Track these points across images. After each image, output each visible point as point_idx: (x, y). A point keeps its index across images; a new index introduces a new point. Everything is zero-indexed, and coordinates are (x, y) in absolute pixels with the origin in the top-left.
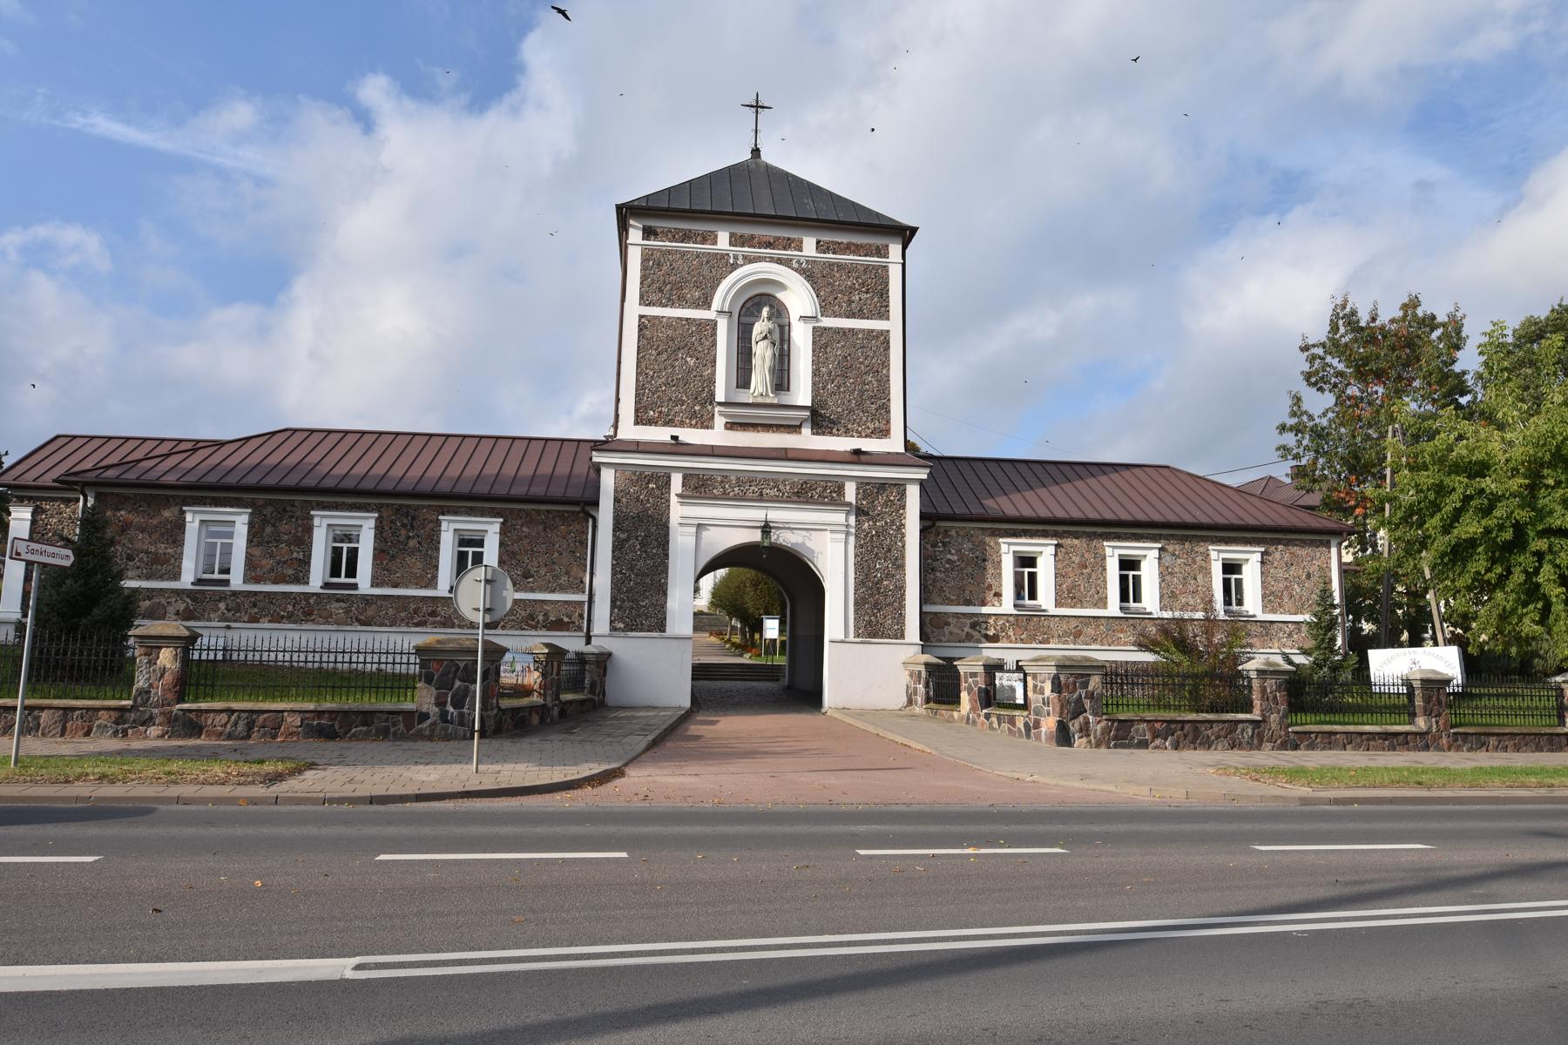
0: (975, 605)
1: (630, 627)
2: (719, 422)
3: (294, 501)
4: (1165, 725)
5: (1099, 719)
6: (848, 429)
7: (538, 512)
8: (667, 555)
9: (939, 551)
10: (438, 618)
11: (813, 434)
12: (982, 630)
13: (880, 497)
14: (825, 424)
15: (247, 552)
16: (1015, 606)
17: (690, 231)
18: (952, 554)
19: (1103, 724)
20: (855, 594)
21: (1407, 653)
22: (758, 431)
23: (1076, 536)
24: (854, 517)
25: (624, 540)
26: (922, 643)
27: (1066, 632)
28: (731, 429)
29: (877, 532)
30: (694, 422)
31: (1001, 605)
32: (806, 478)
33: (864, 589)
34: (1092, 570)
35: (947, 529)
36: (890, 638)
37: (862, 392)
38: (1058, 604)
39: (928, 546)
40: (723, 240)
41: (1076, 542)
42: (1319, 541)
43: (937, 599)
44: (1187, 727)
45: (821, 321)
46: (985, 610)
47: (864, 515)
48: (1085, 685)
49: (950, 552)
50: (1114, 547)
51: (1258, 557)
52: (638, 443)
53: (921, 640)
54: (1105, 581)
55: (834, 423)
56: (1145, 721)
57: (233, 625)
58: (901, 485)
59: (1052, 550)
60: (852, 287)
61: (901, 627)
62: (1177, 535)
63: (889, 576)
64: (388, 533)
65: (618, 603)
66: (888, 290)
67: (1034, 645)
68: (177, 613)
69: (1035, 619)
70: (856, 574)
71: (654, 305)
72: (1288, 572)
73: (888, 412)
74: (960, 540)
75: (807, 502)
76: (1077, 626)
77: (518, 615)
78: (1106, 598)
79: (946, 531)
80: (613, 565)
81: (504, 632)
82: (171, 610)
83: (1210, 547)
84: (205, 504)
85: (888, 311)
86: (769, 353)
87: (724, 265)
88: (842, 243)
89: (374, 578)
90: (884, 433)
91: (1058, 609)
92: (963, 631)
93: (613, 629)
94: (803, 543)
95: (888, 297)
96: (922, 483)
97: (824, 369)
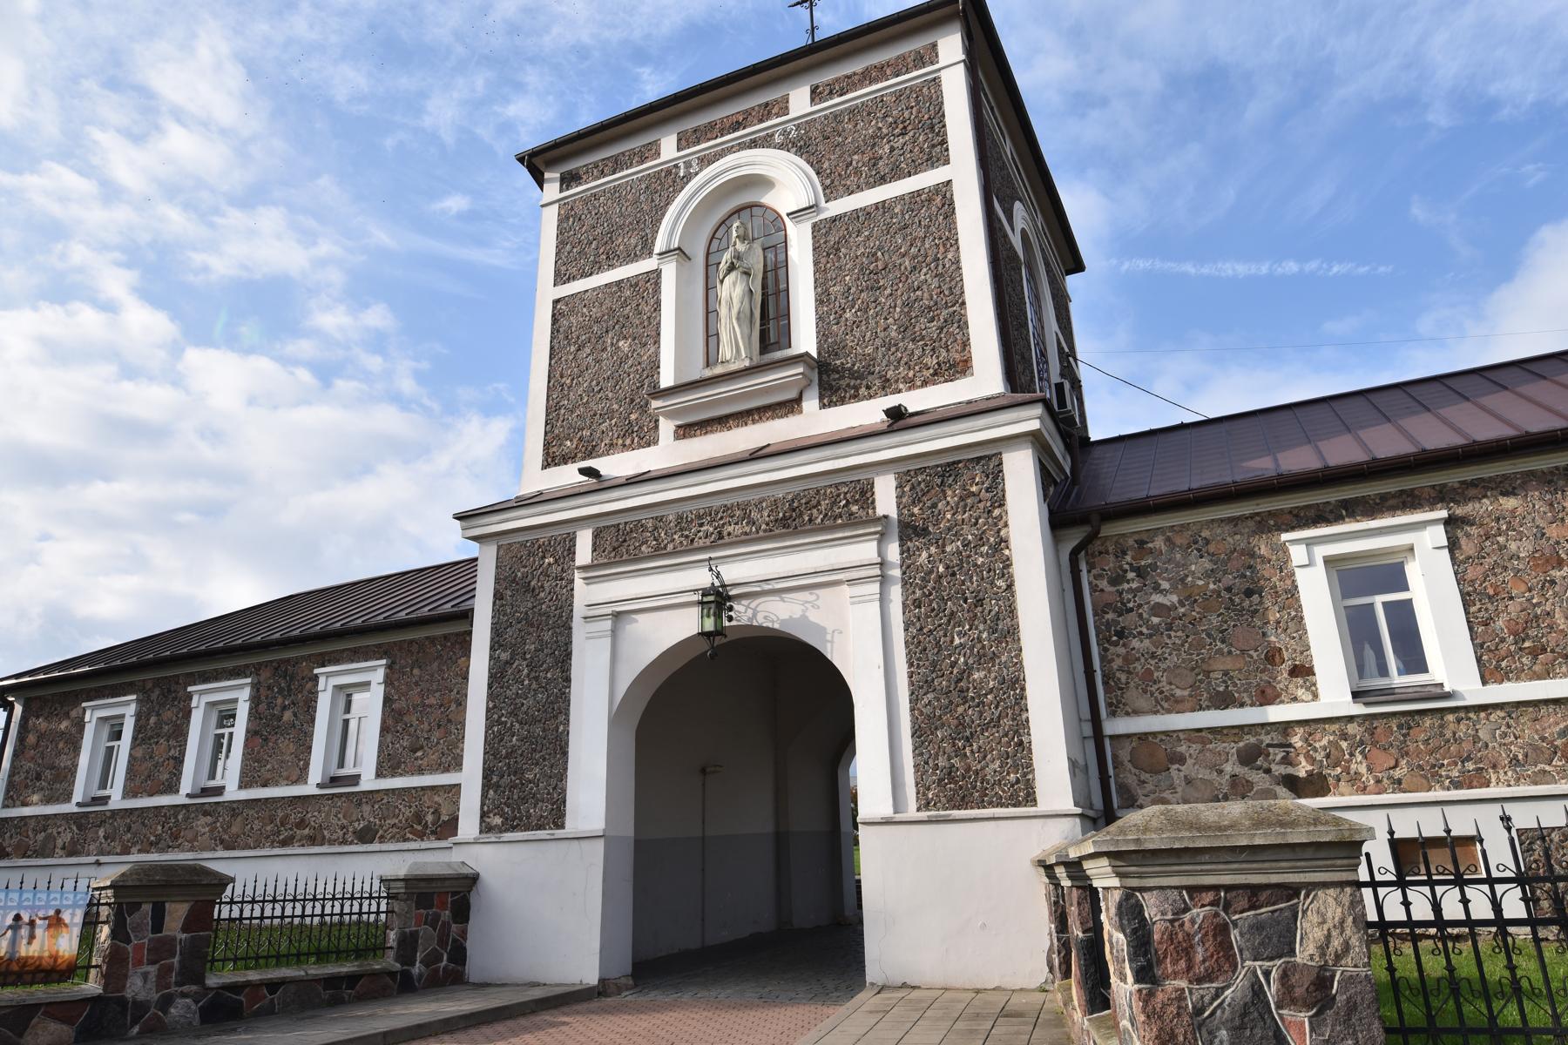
0: (1242, 705)
1: (511, 825)
2: (666, 427)
3: (178, 676)
6: (888, 380)
7: (432, 640)
8: (568, 680)
9: (1130, 590)
10: (306, 831)
11: (823, 406)
12: (1274, 767)
13: (949, 493)
14: (843, 383)
15: (130, 755)
16: (1356, 695)
17: (623, 154)
18: (1161, 592)
20: (912, 710)
22: (730, 429)
23: (1506, 487)
24: (897, 544)
25: (507, 662)
26: (1079, 811)
27: (1536, 749)
28: (684, 437)
29: (947, 567)
30: (628, 442)
31: (1315, 696)
32: (797, 488)
33: (930, 696)
35: (1144, 537)
37: (908, 304)
39: (1103, 584)
40: (669, 147)
41: (1510, 503)
43: (1142, 703)
45: (828, 209)
46: (1276, 713)
47: (918, 535)
48: (1281, 940)
49: (1157, 588)
52: (541, 493)
55: (861, 377)
57: (103, 859)
58: (989, 457)
60: (877, 137)
61: (1025, 775)
63: (985, 658)
64: (262, 707)
65: (495, 779)
66: (943, 116)
68: (63, 848)
69: (1428, 722)
70: (911, 665)
71: (574, 279)
73: (963, 325)
74: (1178, 556)
75: (796, 533)
77: (401, 817)
79: (1141, 543)
80: (488, 710)
81: (384, 847)
82: (59, 842)
84: (103, 696)
85: (947, 150)
86: (739, 291)
87: (670, 181)
88: (855, 74)
89: (243, 774)
90: (960, 367)
92: (1220, 772)
93: (486, 828)
94: (804, 617)
95: (944, 126)
96: (1035, 439)
97: (837, 288)
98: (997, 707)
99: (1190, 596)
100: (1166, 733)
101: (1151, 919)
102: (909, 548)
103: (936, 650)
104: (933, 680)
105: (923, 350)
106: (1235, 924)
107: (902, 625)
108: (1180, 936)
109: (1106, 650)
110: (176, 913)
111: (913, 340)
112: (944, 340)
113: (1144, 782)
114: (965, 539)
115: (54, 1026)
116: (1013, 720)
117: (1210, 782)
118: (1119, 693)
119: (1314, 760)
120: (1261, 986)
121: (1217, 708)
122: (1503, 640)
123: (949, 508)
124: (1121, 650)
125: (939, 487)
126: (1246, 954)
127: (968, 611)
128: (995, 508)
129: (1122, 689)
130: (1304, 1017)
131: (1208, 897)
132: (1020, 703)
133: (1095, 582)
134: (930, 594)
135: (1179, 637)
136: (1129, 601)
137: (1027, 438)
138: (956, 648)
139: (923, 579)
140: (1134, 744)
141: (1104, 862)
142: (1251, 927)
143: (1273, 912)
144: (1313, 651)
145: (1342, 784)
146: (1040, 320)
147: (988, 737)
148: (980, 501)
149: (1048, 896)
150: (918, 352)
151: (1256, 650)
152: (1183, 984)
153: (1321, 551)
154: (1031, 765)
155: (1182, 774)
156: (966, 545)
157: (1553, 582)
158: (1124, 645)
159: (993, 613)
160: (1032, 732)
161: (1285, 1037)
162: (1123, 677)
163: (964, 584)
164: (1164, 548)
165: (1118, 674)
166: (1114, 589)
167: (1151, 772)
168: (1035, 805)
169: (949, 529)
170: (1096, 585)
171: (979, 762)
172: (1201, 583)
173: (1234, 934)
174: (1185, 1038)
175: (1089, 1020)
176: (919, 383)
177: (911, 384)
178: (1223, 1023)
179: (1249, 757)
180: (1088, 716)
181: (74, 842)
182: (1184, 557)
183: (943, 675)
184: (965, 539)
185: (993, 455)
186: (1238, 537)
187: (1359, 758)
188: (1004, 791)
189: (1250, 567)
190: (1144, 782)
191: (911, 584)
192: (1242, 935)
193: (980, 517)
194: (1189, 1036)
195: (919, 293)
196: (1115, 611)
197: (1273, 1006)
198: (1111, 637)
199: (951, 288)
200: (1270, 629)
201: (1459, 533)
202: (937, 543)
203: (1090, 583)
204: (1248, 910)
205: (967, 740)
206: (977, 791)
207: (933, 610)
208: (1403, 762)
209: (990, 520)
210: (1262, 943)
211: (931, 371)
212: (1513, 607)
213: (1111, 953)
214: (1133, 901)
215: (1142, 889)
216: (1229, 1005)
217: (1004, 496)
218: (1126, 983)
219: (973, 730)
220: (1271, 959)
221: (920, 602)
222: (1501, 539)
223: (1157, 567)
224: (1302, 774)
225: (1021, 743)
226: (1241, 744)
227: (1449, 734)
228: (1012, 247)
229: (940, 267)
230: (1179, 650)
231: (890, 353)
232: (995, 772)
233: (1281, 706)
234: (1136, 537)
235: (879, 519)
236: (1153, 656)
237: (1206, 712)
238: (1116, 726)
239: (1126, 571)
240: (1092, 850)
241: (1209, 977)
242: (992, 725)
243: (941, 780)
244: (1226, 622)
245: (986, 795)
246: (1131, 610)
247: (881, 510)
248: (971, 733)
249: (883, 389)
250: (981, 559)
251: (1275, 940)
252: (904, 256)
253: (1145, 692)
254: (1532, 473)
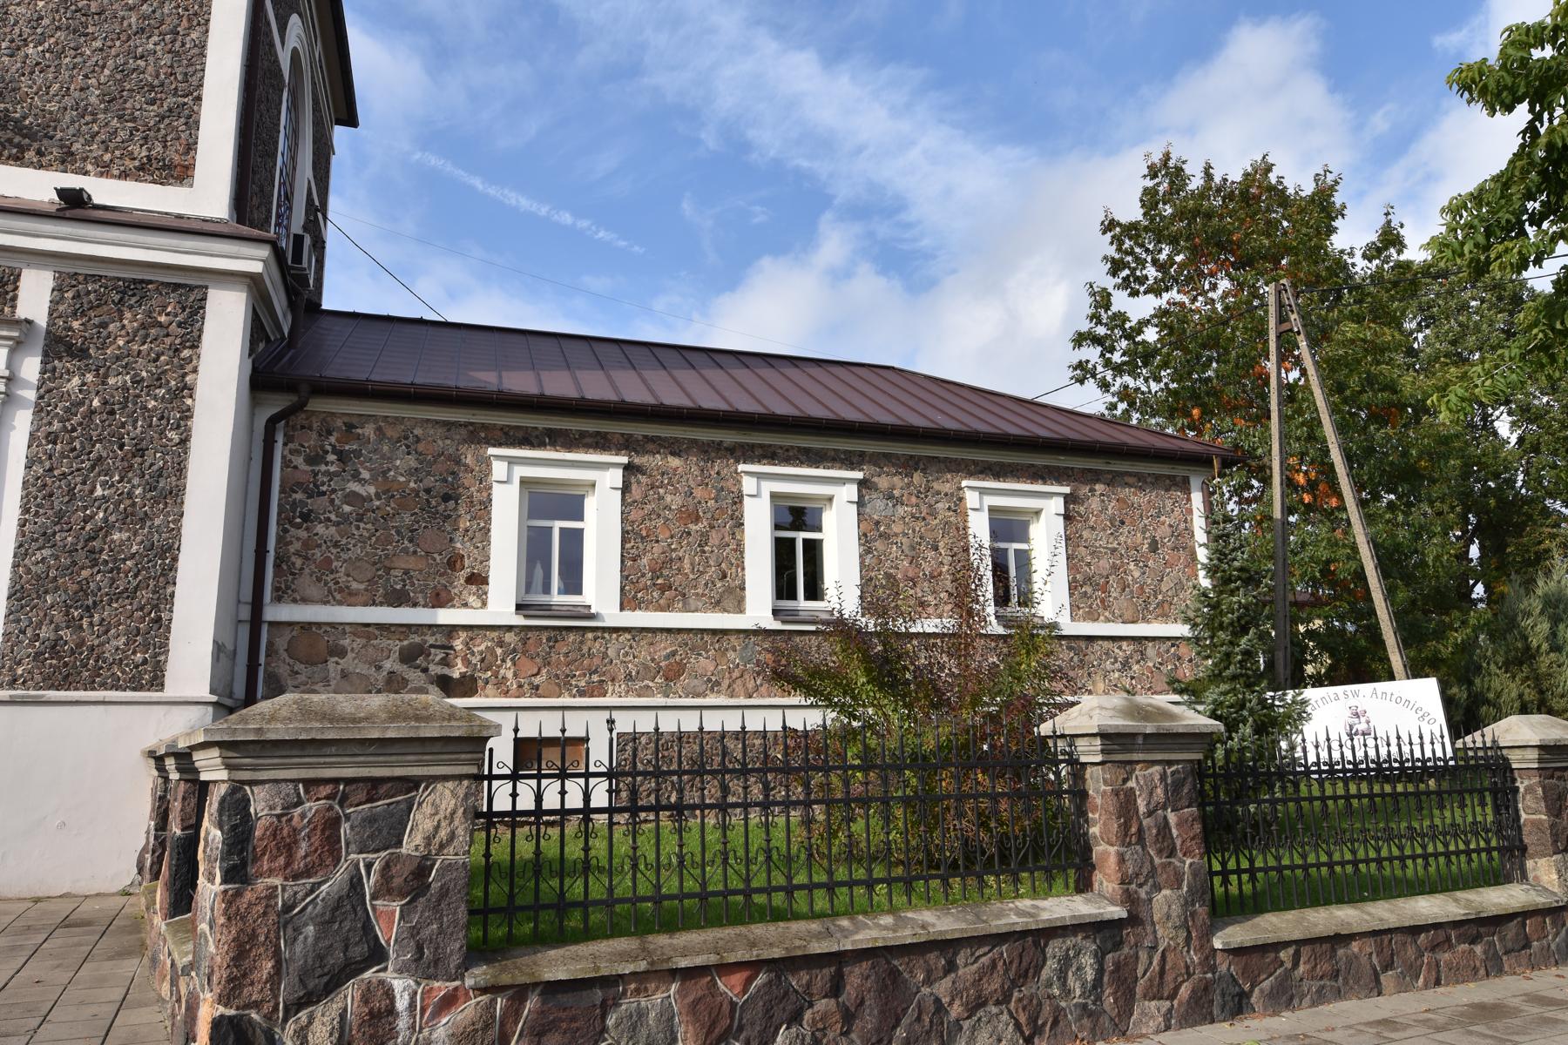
0: (415, 605)
4: (761, 979)
5: (441, 987)
9: (327, 473)
13: (128, 315)
16: (520, 607)
18: (360, 481)
19: (466, 1012)
21: (1341, 696)
23: (675, 448)
24: (39, 359)
26: (214, 698)
27: (646, 667)
29: (105, 403)
31: (484, 604)
33: (46, 552)
34: (712, 527)
35: (355, 421)
36: (116, 687)
38: (628, 602)
39: (299, 461)
41: (674, 462)
42: (1169, 477)
43: (314, 591)
44: (855, 977)
46: (445, 616)
47: (72, 356)
49: (356, 476)
50: (760, 476)
51: (1057, 505)
53: (212, 692)
54: (740, 550)
55: (32, 136)
56: (674, 973)
58: (191, 288)
59: (615, 477)
61: (156, 655)
62: (897, 457)
67: (566, 700)
69: (571, 637)
70: (26, 510)
72: (1116, 538)
73: (193, 124)
74: (386, 448)
76: (674, 653)
78: (743, 589)
79: (350, 427)
83: (964, 483)
90: (178, 172)
91: (627, 613)
92: (379, 668)
96: (253, 283)
97: (21, 10)
98: (136, 576)
99: (388, 491)
100: (332, 625)
101: (256, 814)
102: (54, 369)
103: (67, 498)
104: (54, 534)
105: (131, 134)
106: (348, 817)
107: (24, 461)
108: (285, 832)
109: (286, 531)
111: (120, 117)
112: (163, 132)
113: (297, 673)
114: (136, 375)
116: (154, 592)
117: (367, 677)
118: (290, 578)
119: (470, 662)
120: (361, 878)
121: (390, 605)
122: (643, 575)
123: (123, 333)
124: (303, 534)
125: (116, 304)
126: (353, 847)
127: (123, 460)
128: (185, 348)
129: (294, 574)
130: (396, 906)
131: (326, 790)
132: (168, 574)
133: (289, 457)
134: (74, 430)
135: (368, 530)
136: (323, 484)
137: (244, 280)
138: (95, 500)
139: (67, 410)
140: (294, 633)
141: (215, 752)
142: (364, 820)
143: (389, 805)
144: (492, 563)
145: (489, 686)
146: (293, 158)
147: (116, 609)
148: (168, 335)
149: (154, 790)
150: (123, 135)
151: (440, 554)
152: (277, 881)
153: (521, 471)
154: (167, 645)
155: (339, 667)
156: (138, 382)
157: (689, 534)
158: (307, 529)
159: (155, 468)
160: (175, 609)
161: (373, 927)
162: (299, 562)
163: (123, 427)
164: (372, 436)
165: (293, 559)
166: (310, 468)
167: (307, 663)
168: (162, 690)
169: (118, 358)
170: (290, 461)
171: (98, 637)
172: (402, 479)
173: (345, 829)
174: (267, 938)
175: (167, 925)
176: (116, 172)
177: (105, 170)
178: (312, 919)
179: (409, 657)
180: (249, 599)
182: (391, 451)
183: (70, 530)
184: (136, 375)
185: (197, 287)
186: (448, 442)
187: (509, 664)
188: (124, 672)
189: (453, 473)
190: (297, 673)
191: (48, 413)
192: (352, 828)
193: (163, 354)
194: (272, 935)
195: (141, 63)
196: (305, 492)
197: (368, 898)
198: (294, 518)
199: (186, 74)
200: (458, 536)
201: (633, 480)
202: (97, 370)
203: (283, 457)
204: (365, 803)
205: (88, 609)
206: (88, 670)
207: (75, 449)
208: (544, 671)
209: (176, 360)
210: (371, 837)
211: (137, 163)
212: (657, 549)
213: (204, 852)
214: (239, 795)
215: (252, 783)
216: (323, 900)
217: (200, 336)
218: (213, 883)
219: (98, 599)
220: (377, 851)
221: (57, 437)
222: (661, 491)
223: (361, 455)
224: (456, 675)
225: (158, 620)
226: (406, 643)
227: (585, 649)
228: (276, 61)
229: (178, 44)
230: (365, 542)
231: (83, 121)
232: (117, 649)
233: (452, 610)
234: (346, 419)
235: (18, 322)
236: (336, 545)
237: (379, 608)
238: (277, 612)
239: (327, 452)
240: (201, 740)
241: (307, 873)
242: (125, 595)
243: (38, 654)
244: (418, 522)
245: (99, 675)
246: (324, 493)
247: (22, 312)
248: (94, 602)
249: (63, 162)
250: (153, 403)
251: (385, 832)
252: (131, 9)
253: (319, 580)
254: (695, 441)
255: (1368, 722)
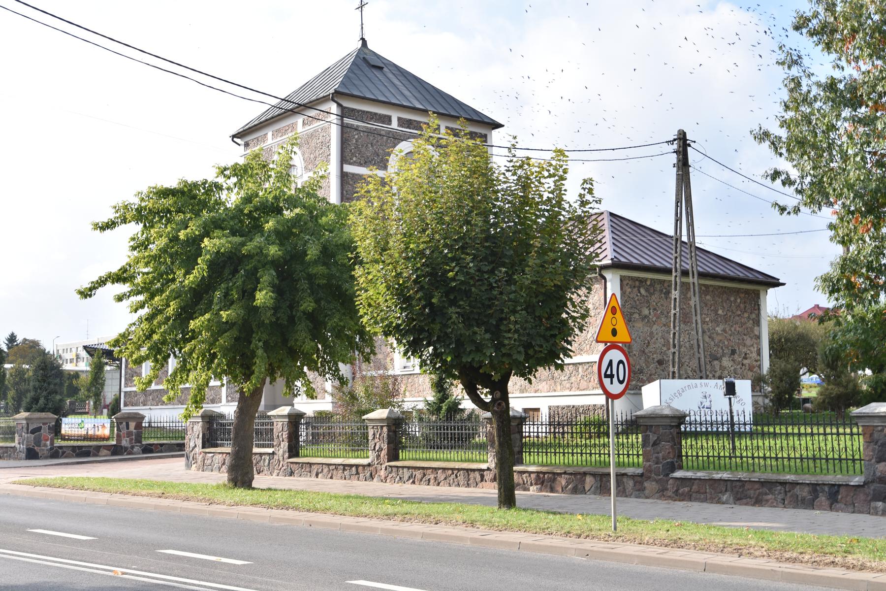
21: (699, 385)
57: (152, 407)
110: (132, 425)
115: (105, 451)
181: (144, 401)
255: (711, 401)
